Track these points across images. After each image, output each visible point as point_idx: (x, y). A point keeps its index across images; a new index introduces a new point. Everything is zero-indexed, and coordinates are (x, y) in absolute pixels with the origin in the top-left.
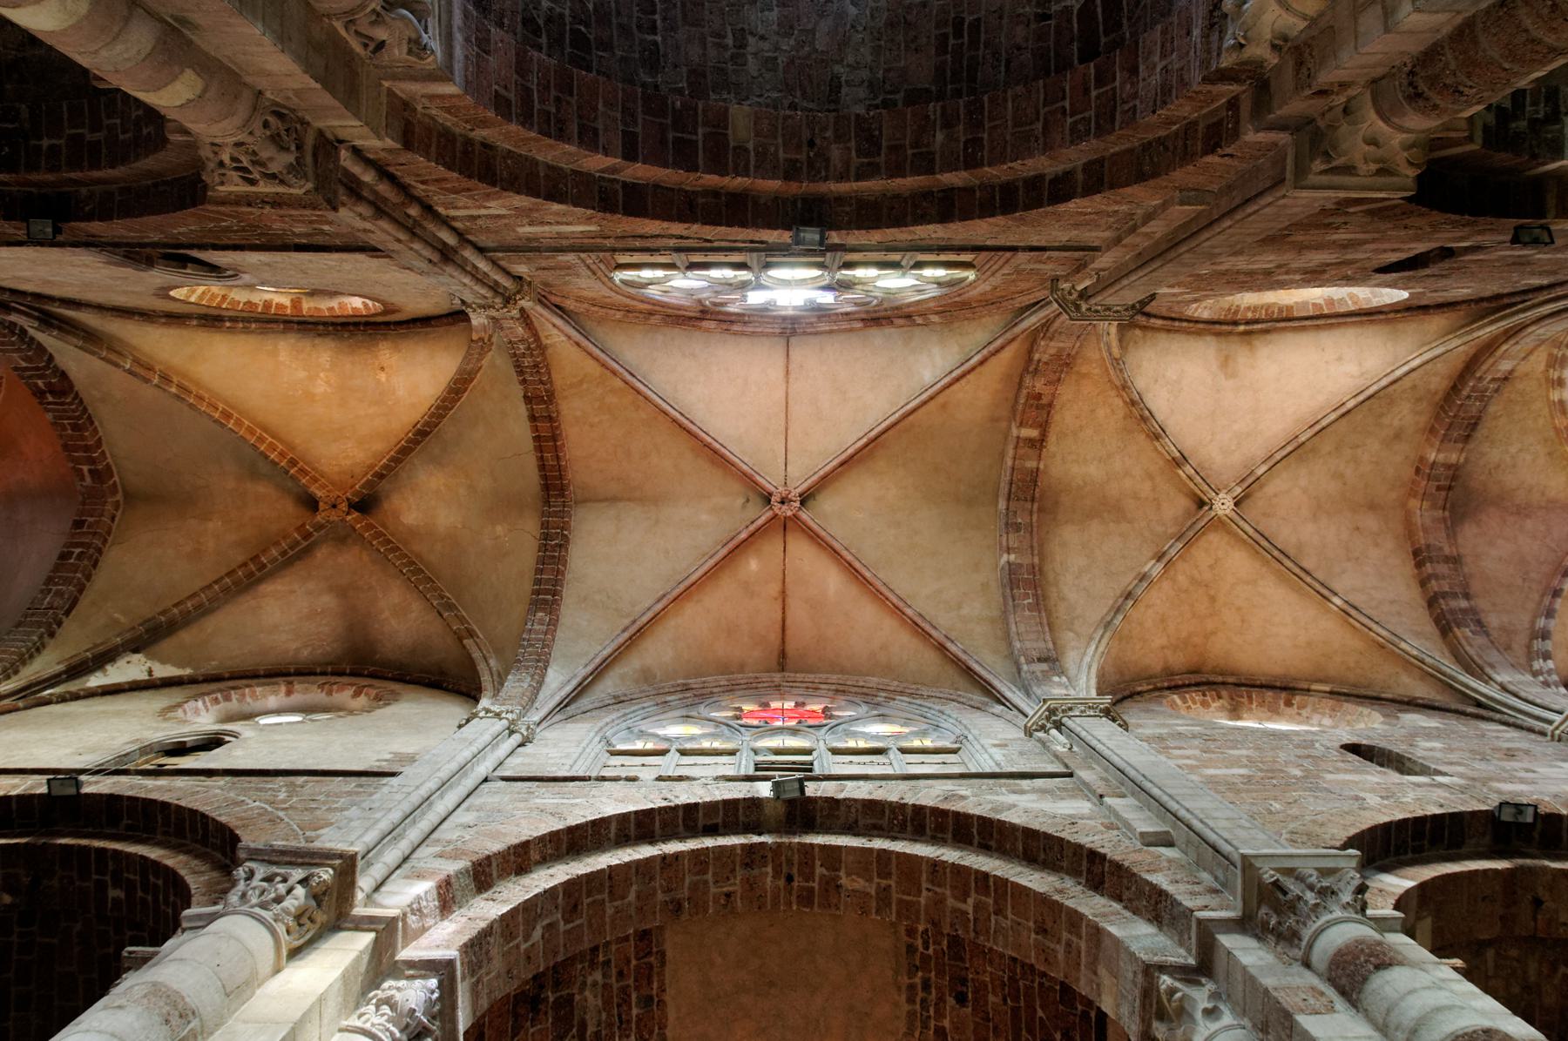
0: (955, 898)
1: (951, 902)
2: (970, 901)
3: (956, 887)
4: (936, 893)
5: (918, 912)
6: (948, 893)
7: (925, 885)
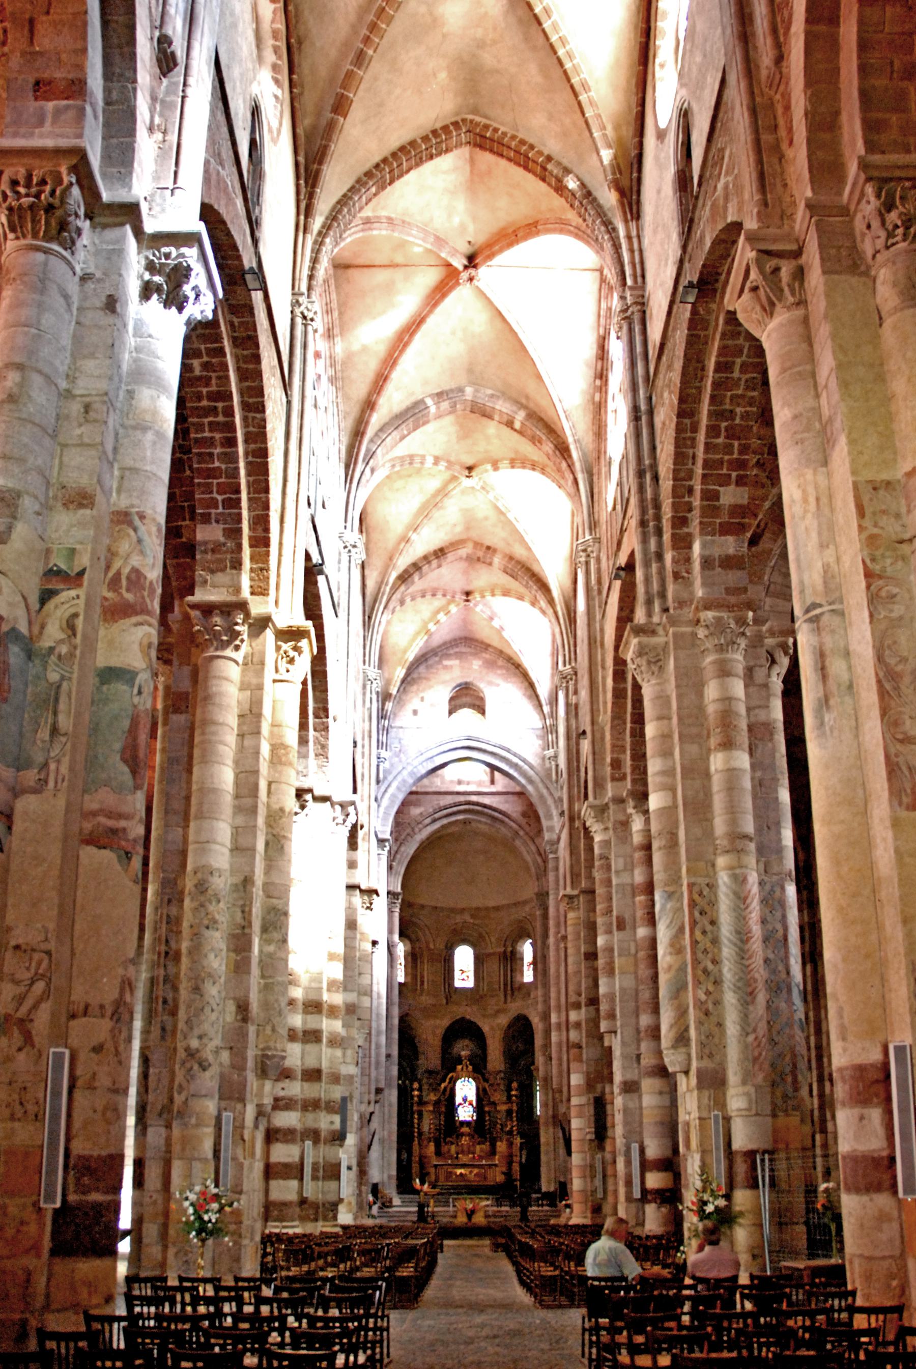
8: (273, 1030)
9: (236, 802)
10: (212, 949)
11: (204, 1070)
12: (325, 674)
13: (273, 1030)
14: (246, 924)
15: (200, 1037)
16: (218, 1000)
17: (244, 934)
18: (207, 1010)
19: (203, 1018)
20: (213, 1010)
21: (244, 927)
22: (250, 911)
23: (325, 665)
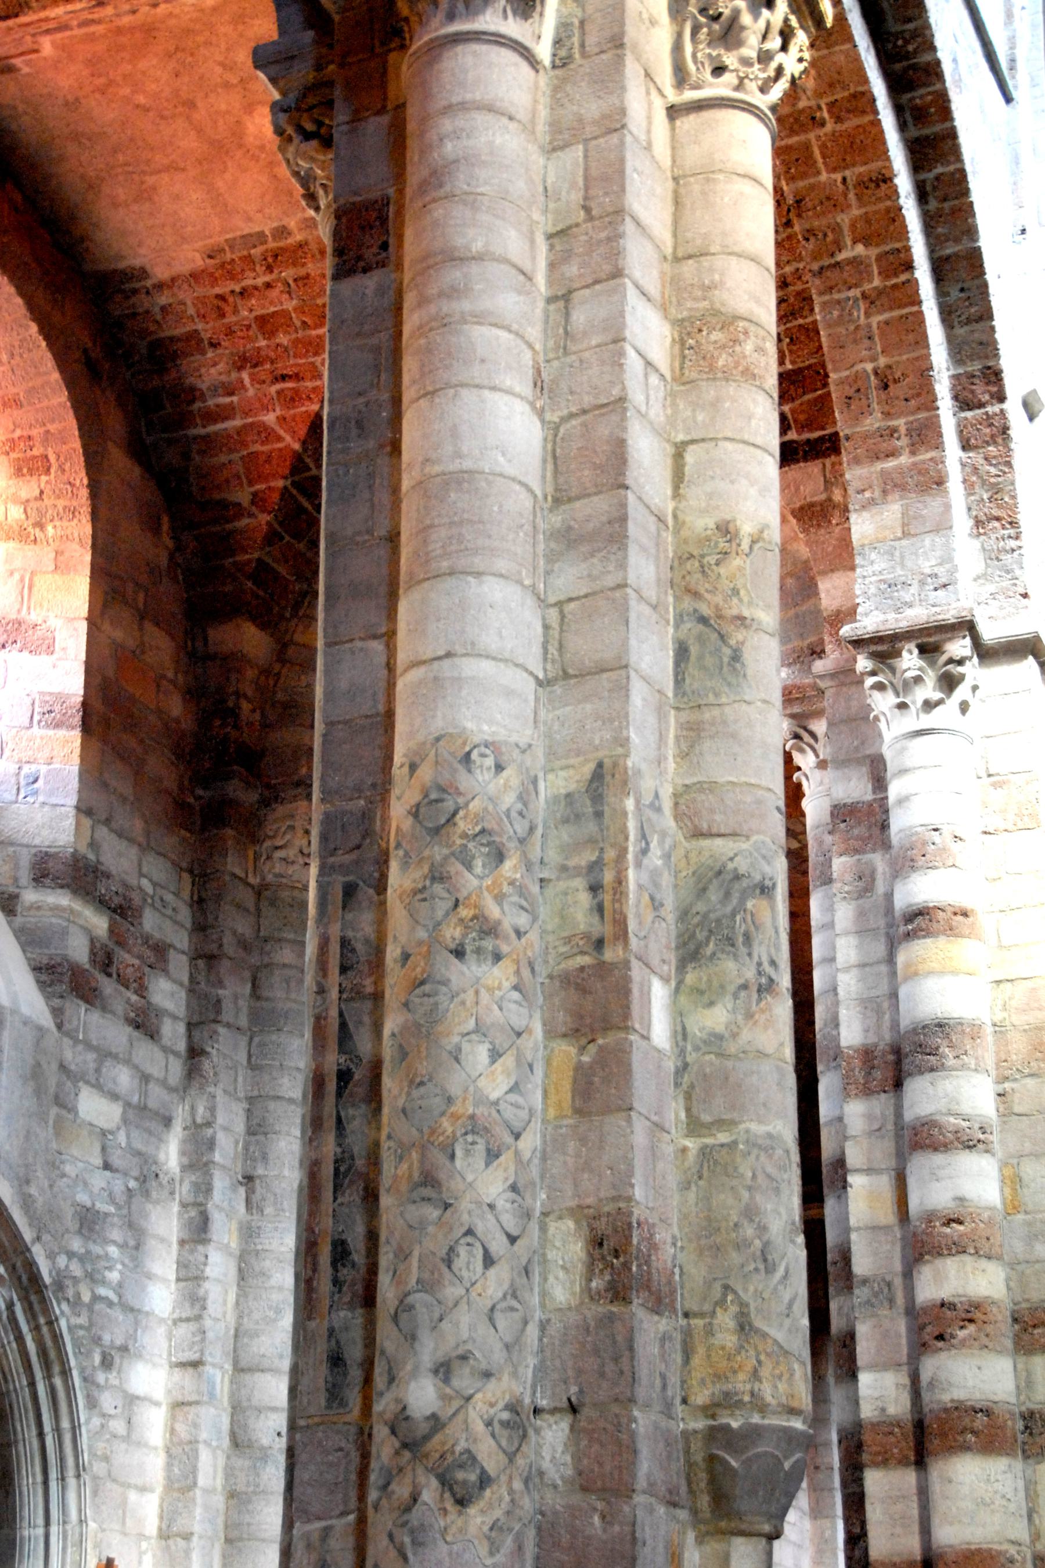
0: (853, 226)
1: (844, 219)
2: (860, 249)
3: (868, 222)
4: (845, 195)
5: (804, 175)
6: (856, 212)
7: (847, 173)
8: (744, 1326)
9: (557, 520)
10: (479, 1030)
11: (462, 1502)
12: (974, 261)
13: (744, 1326)
14: (608, 930)
15: (444, 1370)
16: (511, 1224)
17: (602, 969)
18: (470, 1261)
19: (452, 1291)
20: (489, 1261)
21: (599, 944)
22: (620, 881)
23: (971, 232)
